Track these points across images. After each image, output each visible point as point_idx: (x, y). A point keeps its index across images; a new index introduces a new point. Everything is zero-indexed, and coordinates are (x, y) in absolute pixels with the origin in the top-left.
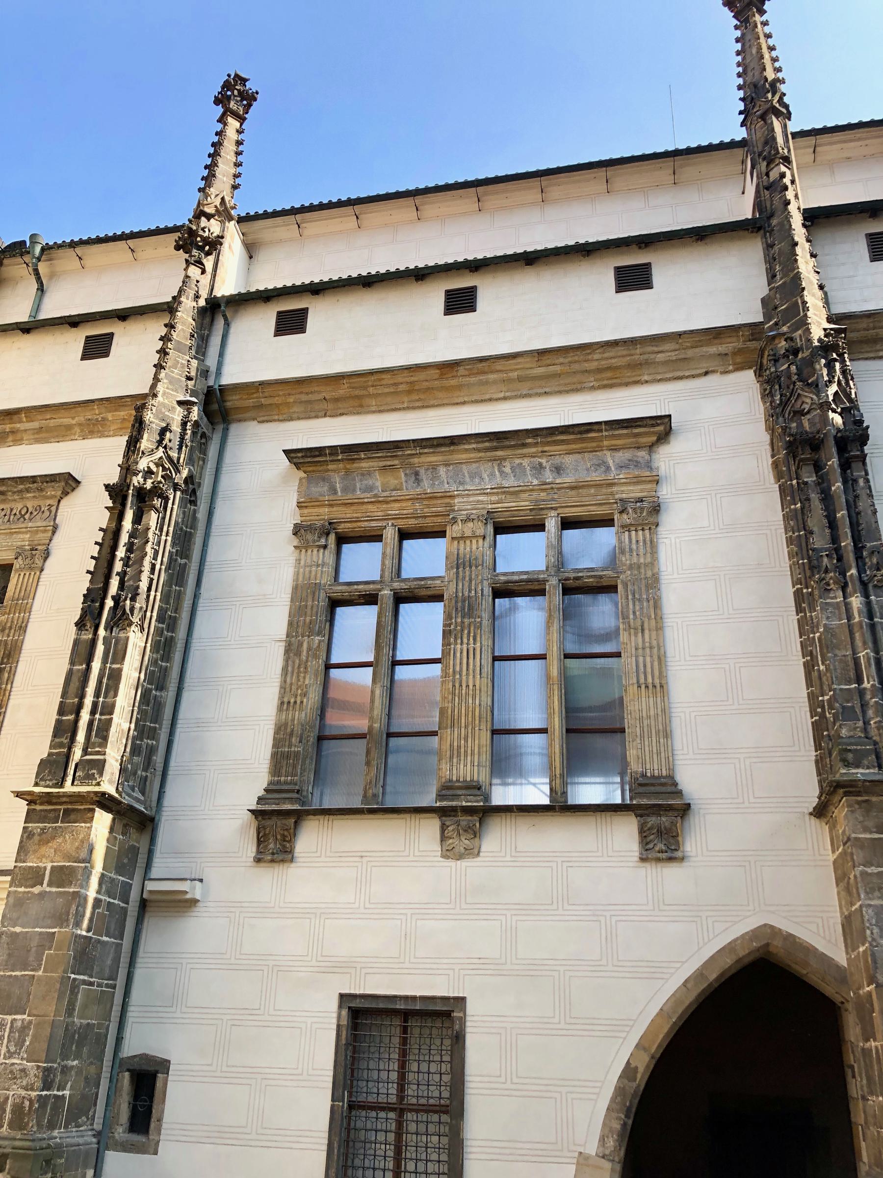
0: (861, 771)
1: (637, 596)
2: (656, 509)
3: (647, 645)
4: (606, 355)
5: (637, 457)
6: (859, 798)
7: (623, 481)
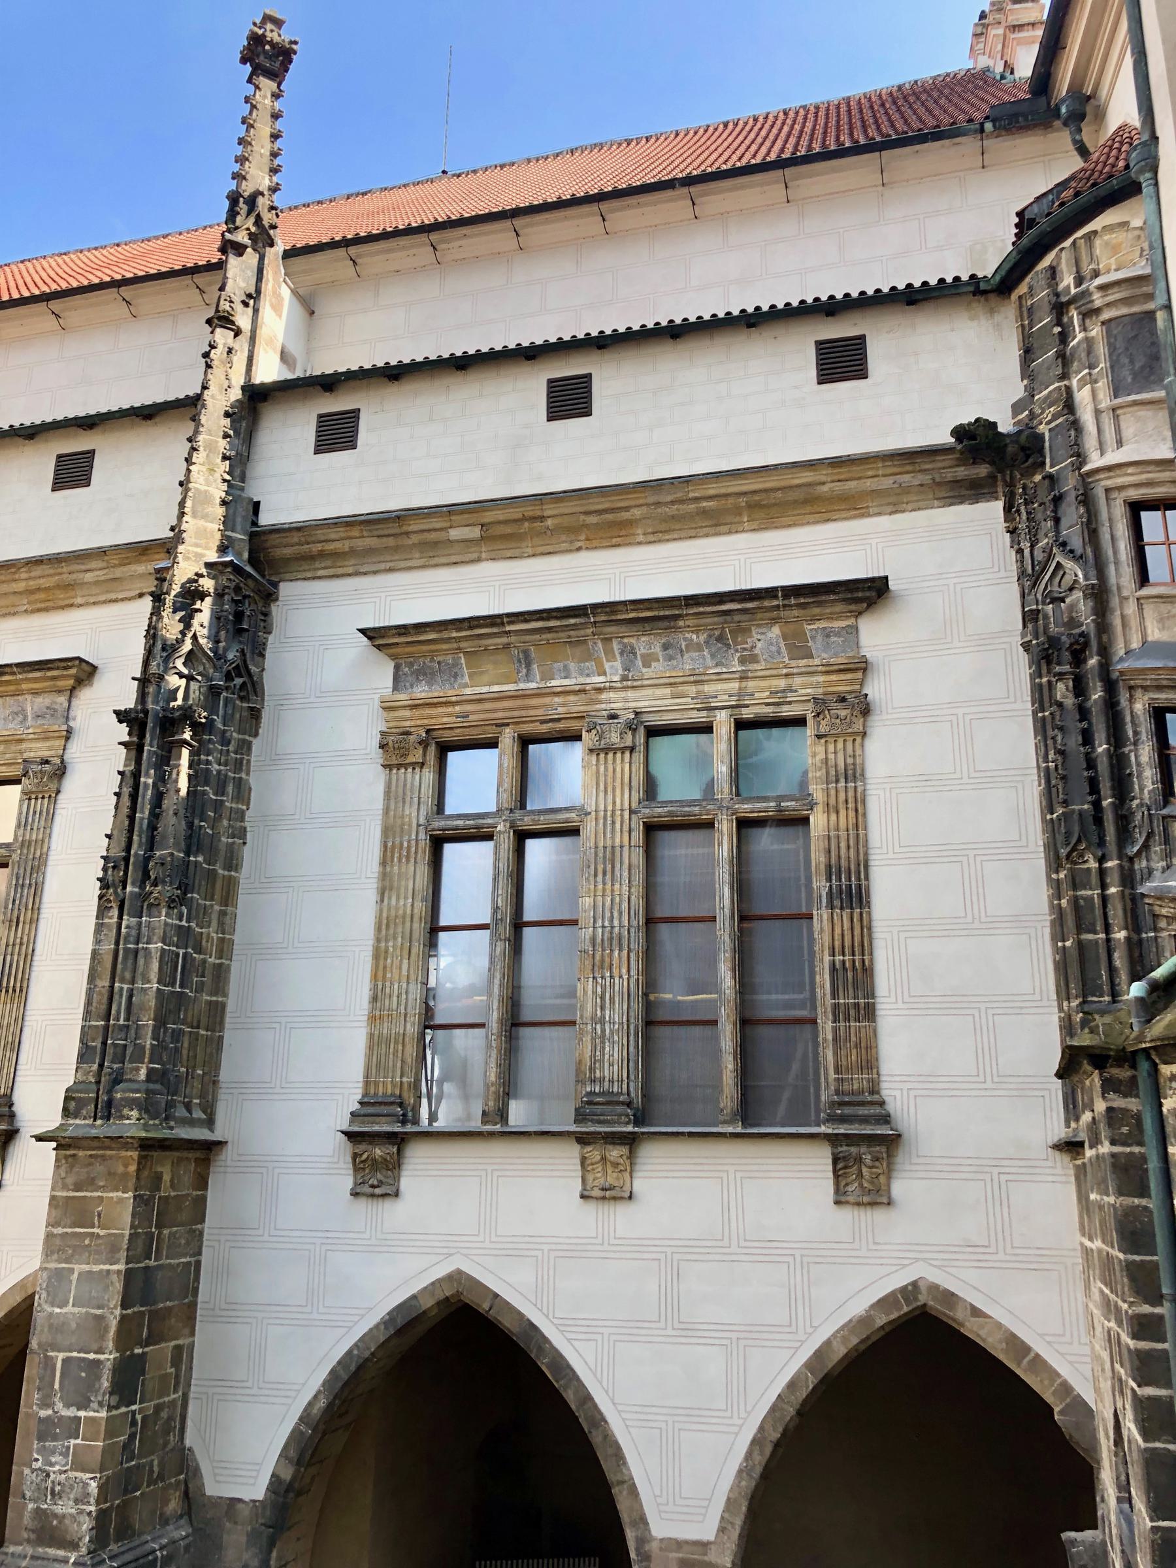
0: (78, 1121)
1: (21, 882)
2: (61, 772)
3: (18, 941)
4: (33, 574)
5: (56, 703)
6: (68, 1153)
7: (32, 736)
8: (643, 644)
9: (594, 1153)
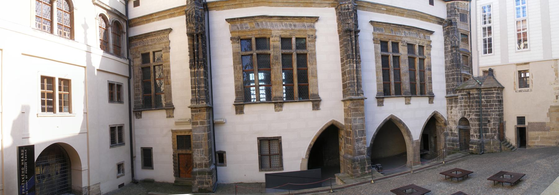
8: (407, 32)
9: (407, 98)
